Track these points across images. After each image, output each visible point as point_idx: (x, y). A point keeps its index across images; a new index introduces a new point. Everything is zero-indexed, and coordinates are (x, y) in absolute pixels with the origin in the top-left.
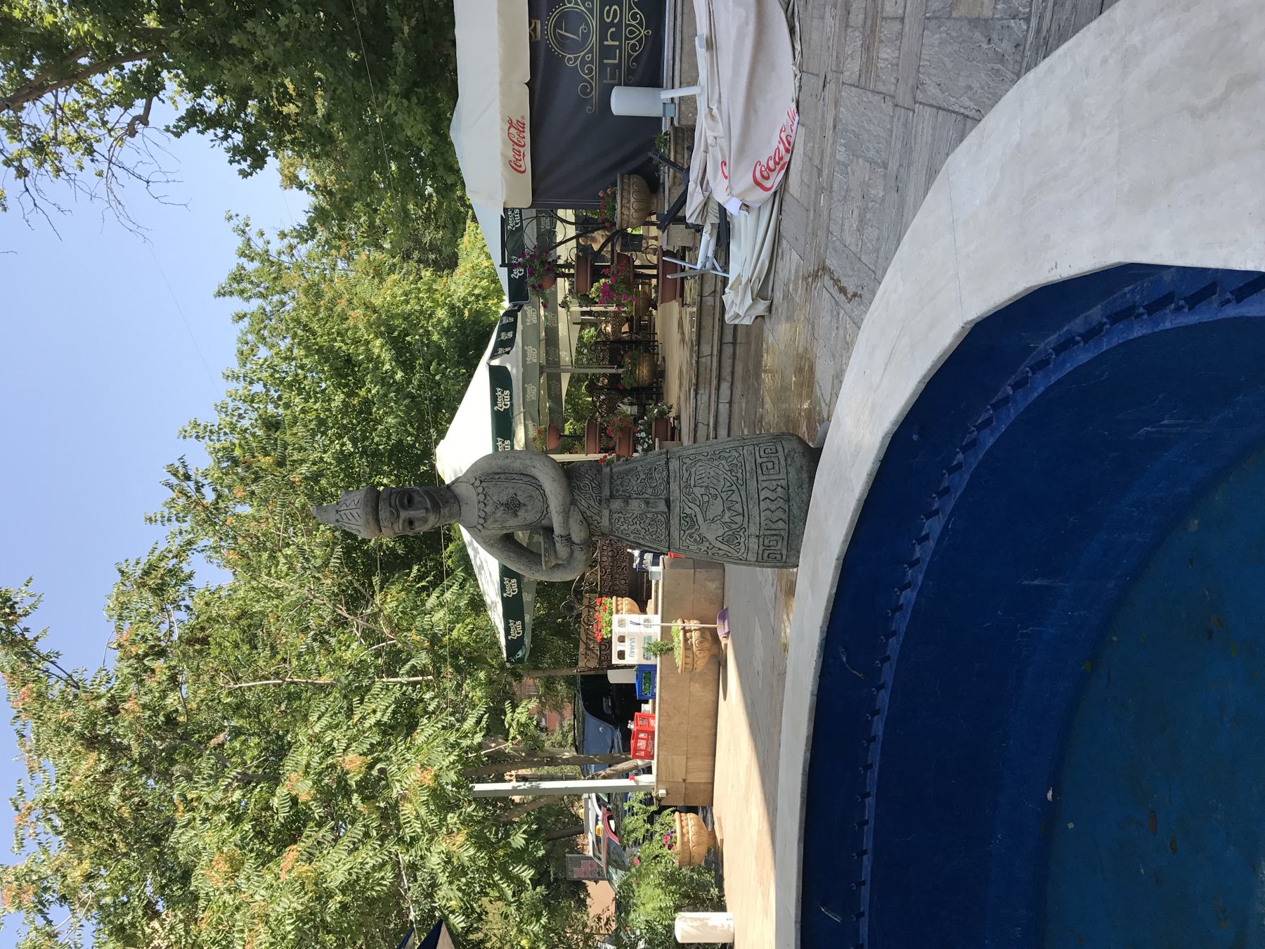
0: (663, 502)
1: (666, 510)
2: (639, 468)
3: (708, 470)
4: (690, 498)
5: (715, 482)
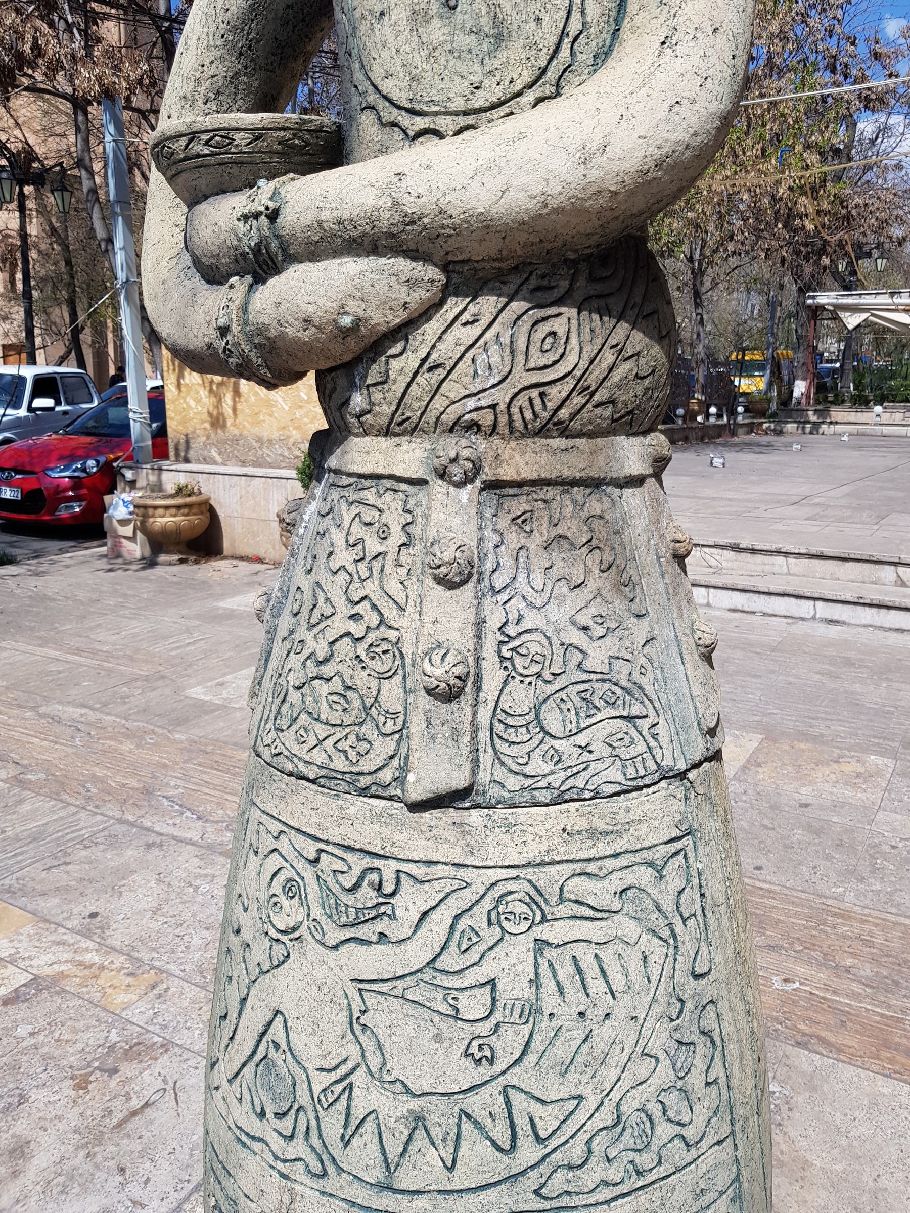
0: (459, 781)
1: (416, 794)
2: (640, 630)
3: (619, 1013)
4: (477, 919)
5: (561, 1051)
